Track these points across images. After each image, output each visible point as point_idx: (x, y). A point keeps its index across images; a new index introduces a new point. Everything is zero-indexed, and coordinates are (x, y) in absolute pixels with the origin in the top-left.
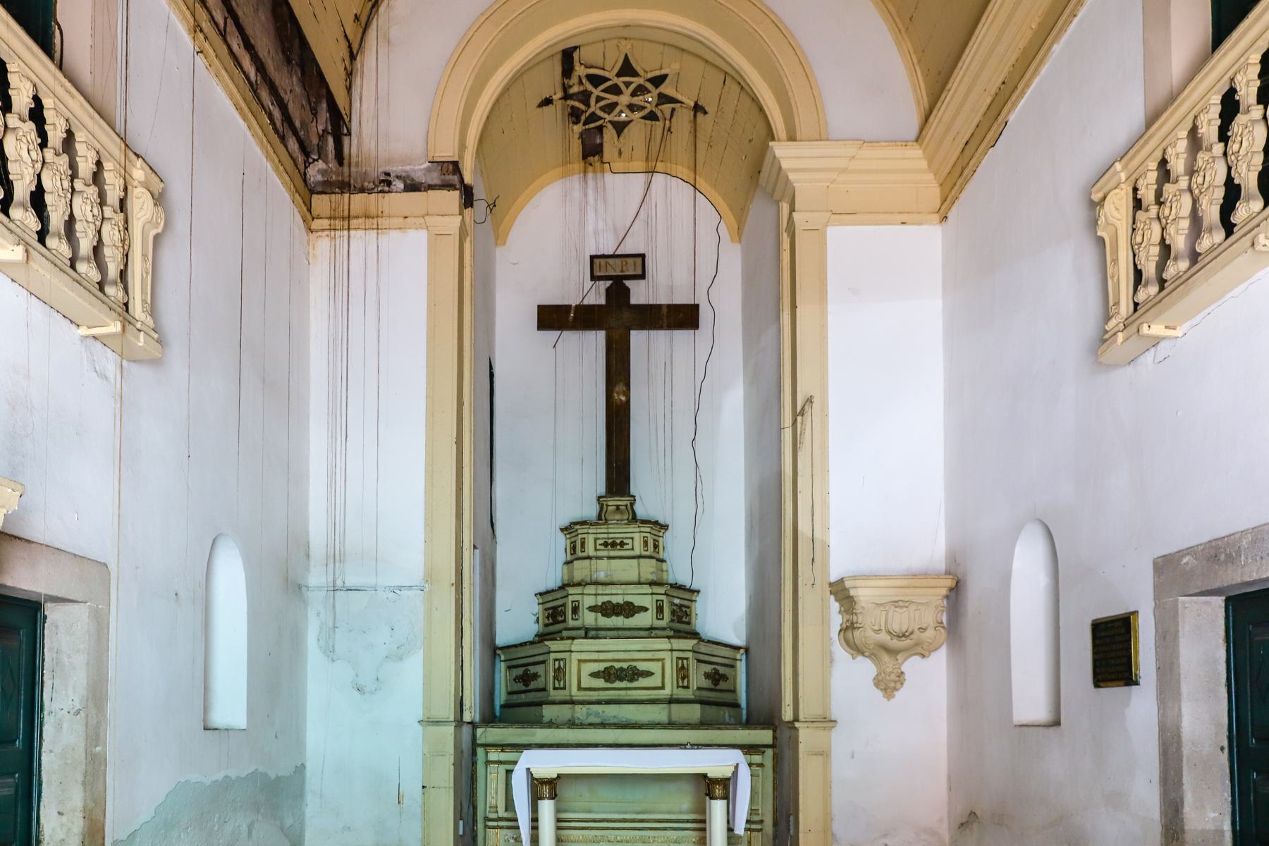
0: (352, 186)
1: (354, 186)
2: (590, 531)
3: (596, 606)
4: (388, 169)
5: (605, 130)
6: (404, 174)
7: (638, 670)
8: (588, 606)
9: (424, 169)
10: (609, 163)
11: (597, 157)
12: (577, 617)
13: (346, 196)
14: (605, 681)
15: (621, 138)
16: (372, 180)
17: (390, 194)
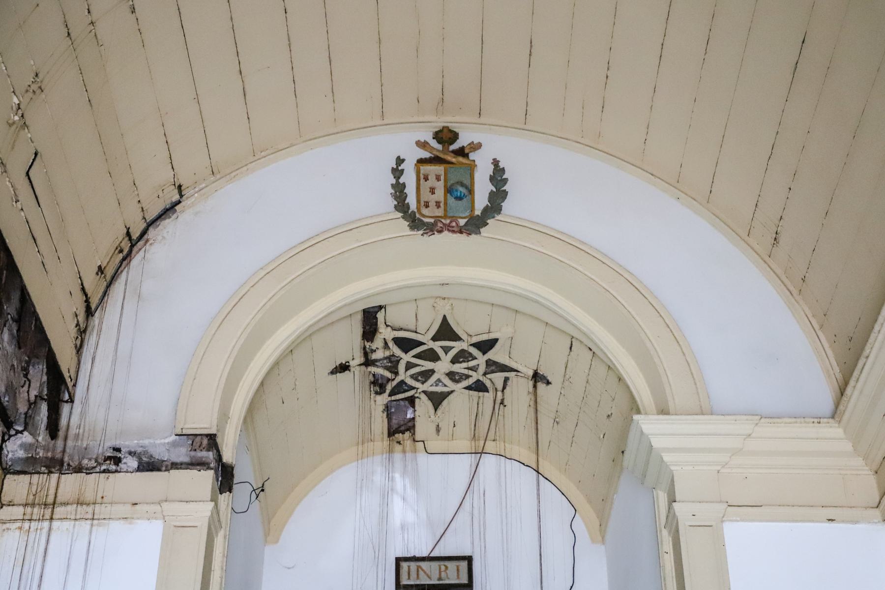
0: (65, 464)
1: (69, 465)
4: (118, 443)
5: (417, 401)
6: (139, 450)
9: (168, 443)
10: (423, 441)
11: (407, 434)
13: (55, 476)
15: (439, 412)
16: (94, 457)
17: (117, 475)
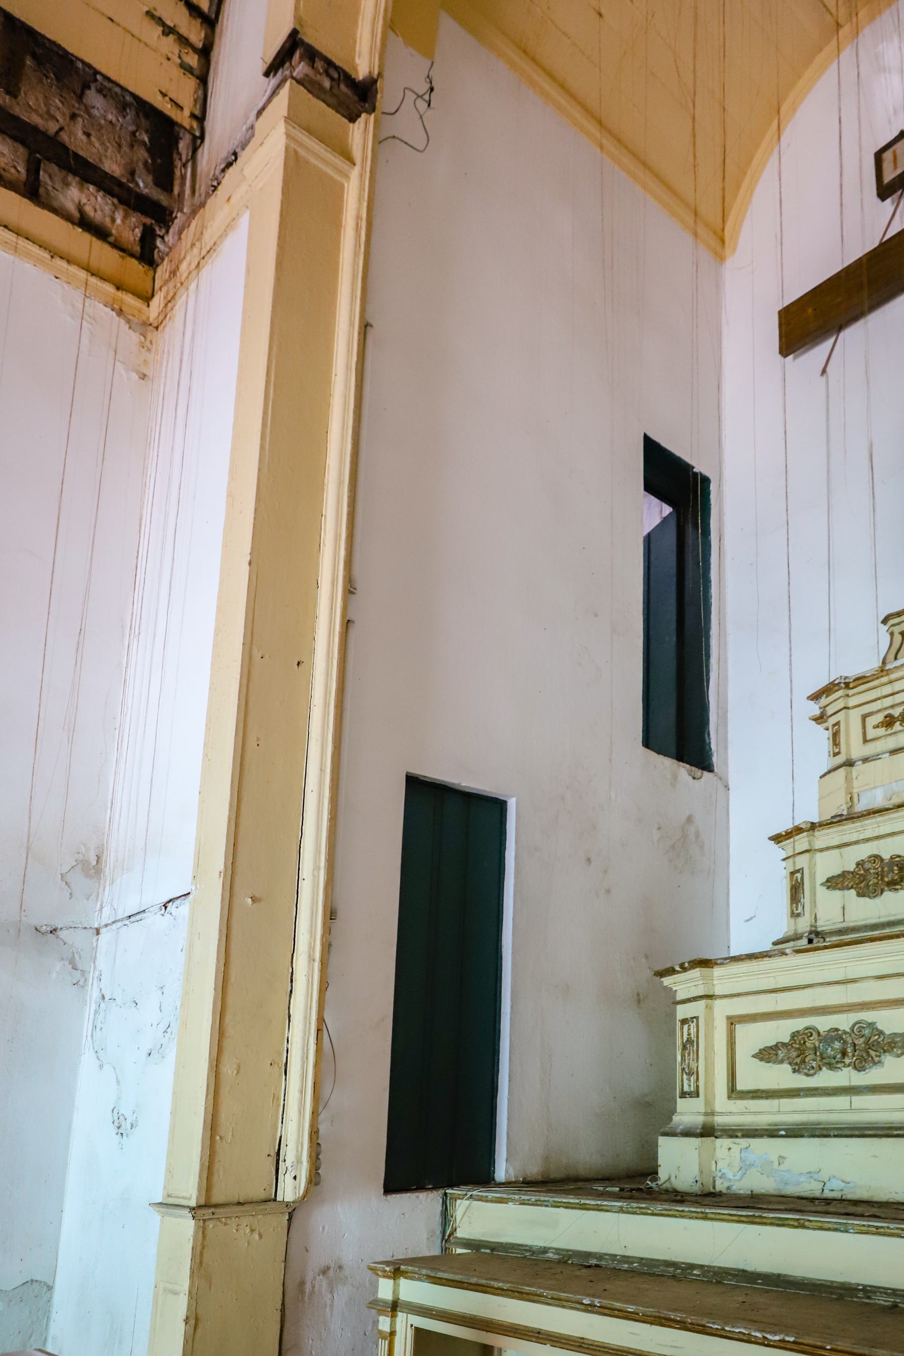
2: (852, 702)
3: (844, 874)
7: (881, 1033)
8: (825, 880)
12: (799, 911)
14: (794, 1071)
